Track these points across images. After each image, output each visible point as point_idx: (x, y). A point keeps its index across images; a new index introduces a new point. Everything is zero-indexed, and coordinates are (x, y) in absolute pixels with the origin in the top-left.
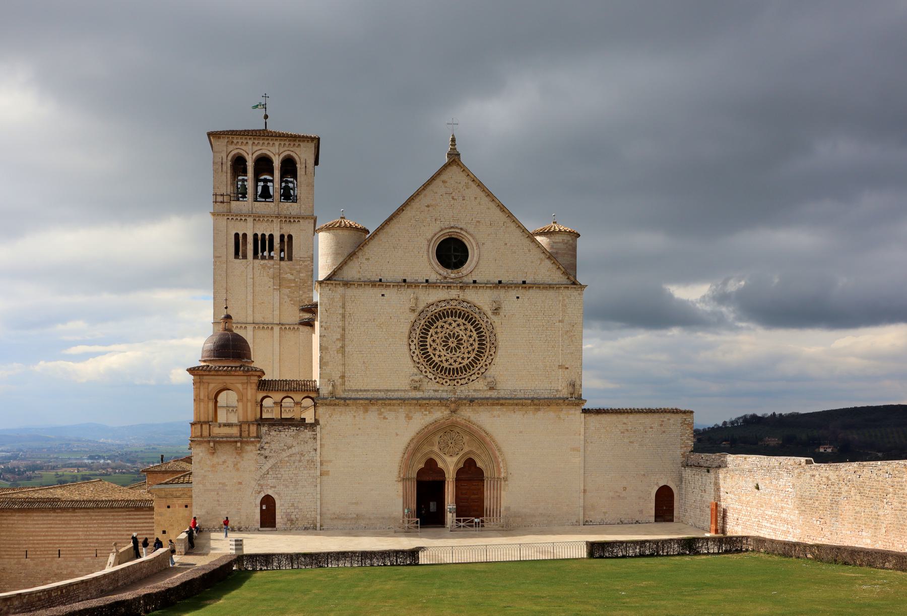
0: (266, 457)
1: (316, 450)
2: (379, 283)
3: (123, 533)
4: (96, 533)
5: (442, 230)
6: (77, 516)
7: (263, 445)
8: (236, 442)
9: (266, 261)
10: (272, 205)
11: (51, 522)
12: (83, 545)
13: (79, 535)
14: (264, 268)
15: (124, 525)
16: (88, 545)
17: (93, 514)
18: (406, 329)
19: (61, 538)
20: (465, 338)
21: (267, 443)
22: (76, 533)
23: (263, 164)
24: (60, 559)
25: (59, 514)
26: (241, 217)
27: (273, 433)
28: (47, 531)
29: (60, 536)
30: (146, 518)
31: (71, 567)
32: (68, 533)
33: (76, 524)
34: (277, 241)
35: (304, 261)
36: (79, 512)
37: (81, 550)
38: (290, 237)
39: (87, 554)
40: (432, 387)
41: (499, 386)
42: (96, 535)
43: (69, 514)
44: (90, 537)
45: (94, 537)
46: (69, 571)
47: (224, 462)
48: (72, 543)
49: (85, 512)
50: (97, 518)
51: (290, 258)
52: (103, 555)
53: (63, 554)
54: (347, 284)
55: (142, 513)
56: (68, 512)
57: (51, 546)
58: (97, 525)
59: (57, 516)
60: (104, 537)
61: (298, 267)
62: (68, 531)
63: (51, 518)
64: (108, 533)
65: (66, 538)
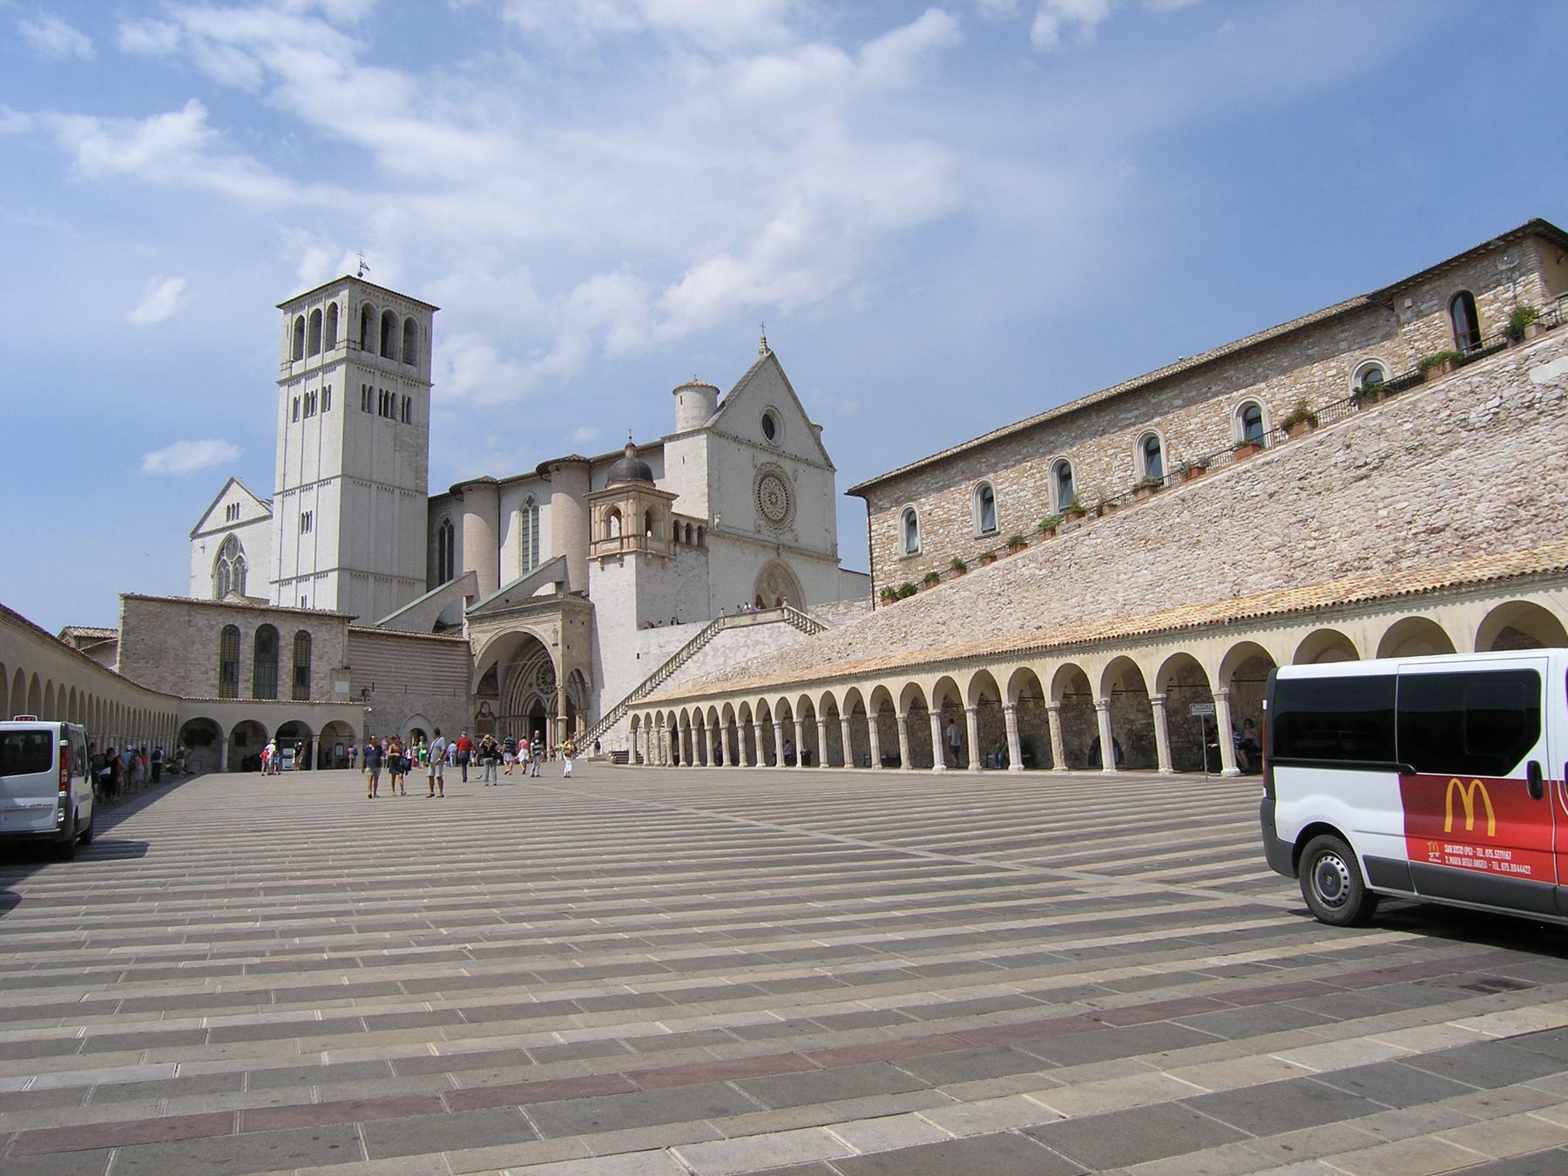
0: (679, 575)
1: (708, 574)
2: (736, 439)
5: (771, 406)
6: (389, 645)
8: (663, 557)
9: (389, 420)
10: (396, 363)
11: (365, 649)
12: (395, 679)
13: (391, 667)
14: (387, 426)
15: (429, 660)
17: (402, 644)
18: (751, 480)
19: (375, 669)
20: (779, 496)
22: (388, 664)
23: (388, 320)
25: (374, 642)
26: (369, 368)
27: (683, 554)
28: (363, 660)
29: (376, 666)
30: (448, 654)
31: (384, 703)
32: (382, 664)
33: (389, 654)
34: (399, 401)
35: (422, 427)
37: (392, 684)
38: (409, 399)
40: (767, 534)
41: (799, 540)
43: (383, 643)
44: (400, 671)
46: (381, 708)
47: (655, 575)
48: (384, 676)
51: (409, 422)
54: (721, 435)
56: (382, 640)
57: (366, 677)
58: (405, 658)
59: (372, 644)
60: (414, 672)
61: (416, 432)
62: (381, 662)
63: (366, 645)
64: (416, 667)
65: (378, 669)
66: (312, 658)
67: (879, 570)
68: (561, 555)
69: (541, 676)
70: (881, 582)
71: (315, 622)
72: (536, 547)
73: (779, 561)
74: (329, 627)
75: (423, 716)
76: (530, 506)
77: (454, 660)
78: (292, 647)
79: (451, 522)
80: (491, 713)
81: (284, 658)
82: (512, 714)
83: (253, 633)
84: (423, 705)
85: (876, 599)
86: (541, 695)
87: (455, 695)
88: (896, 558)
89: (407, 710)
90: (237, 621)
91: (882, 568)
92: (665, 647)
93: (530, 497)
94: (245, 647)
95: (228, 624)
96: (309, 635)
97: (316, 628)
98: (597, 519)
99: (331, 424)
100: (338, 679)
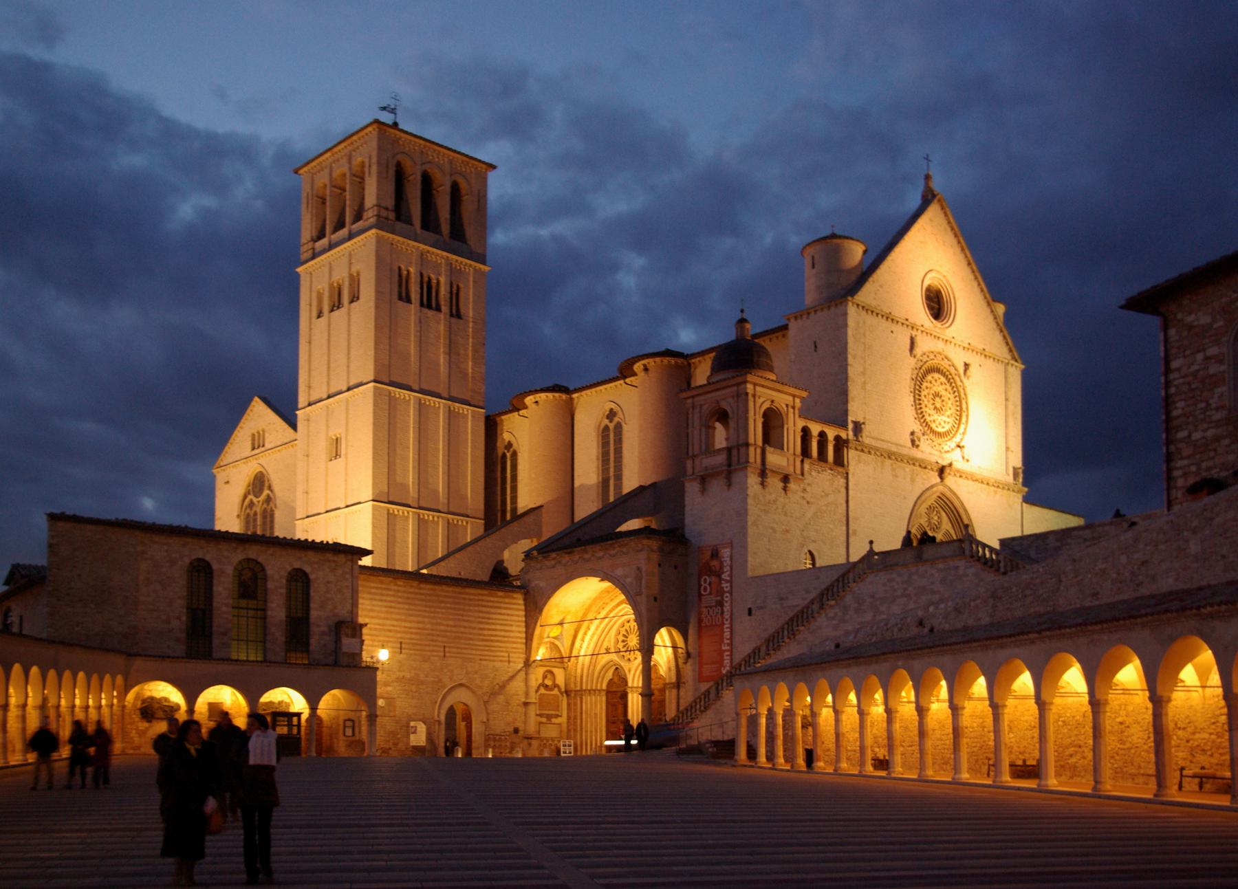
3: (474, 625)
4: (445, 622)
7: (806, 486)
16: (435, 638)
17: (440, 593)
21: (808, 484)
24: (402, 656)
25: (400, 588)
36: (424, 589)
39: (433, 651)
42: (443, 625)
43: (412, 590)
44: (438, 627)
45: (442, 628)
49: (432, 589)
50: (445, 599)
52: (452, 655)
53: (405, 649)
55: (496, 599)
56: (412, 587)
58: (444, 611)
59: (398, 591)
60: (454, 629)
66: (312, 605)
67: (1182, 440)
68: (650, 482)
69: (621, 638)
70: (1185, 462)
71: (312, 556)
72: (619, 477)
73: (941, 488)
74: (333, 565)
75: (468, 687)
76: (611, 422)
77: (508, 615)
78: (283, 591)
79: (515, 446)
80: (556, 686)
81: (274, 605)
82: (584, 688)
83: (230, 570)
84: (467, 673)
85: (1174, 492)
86: (622, 664)
87: (509, 662)
88: (1218, 416)
89: (446, 680)
90: (209, 553)
91: (1189, 436)
92: (787, 598)
93: (611, 410)
94: (220, 589)
95: (194, 557)
96: (305, 574)
97: (316, 566)
98: (697, 424)
99: (361, 317)
100: (347, 636)
